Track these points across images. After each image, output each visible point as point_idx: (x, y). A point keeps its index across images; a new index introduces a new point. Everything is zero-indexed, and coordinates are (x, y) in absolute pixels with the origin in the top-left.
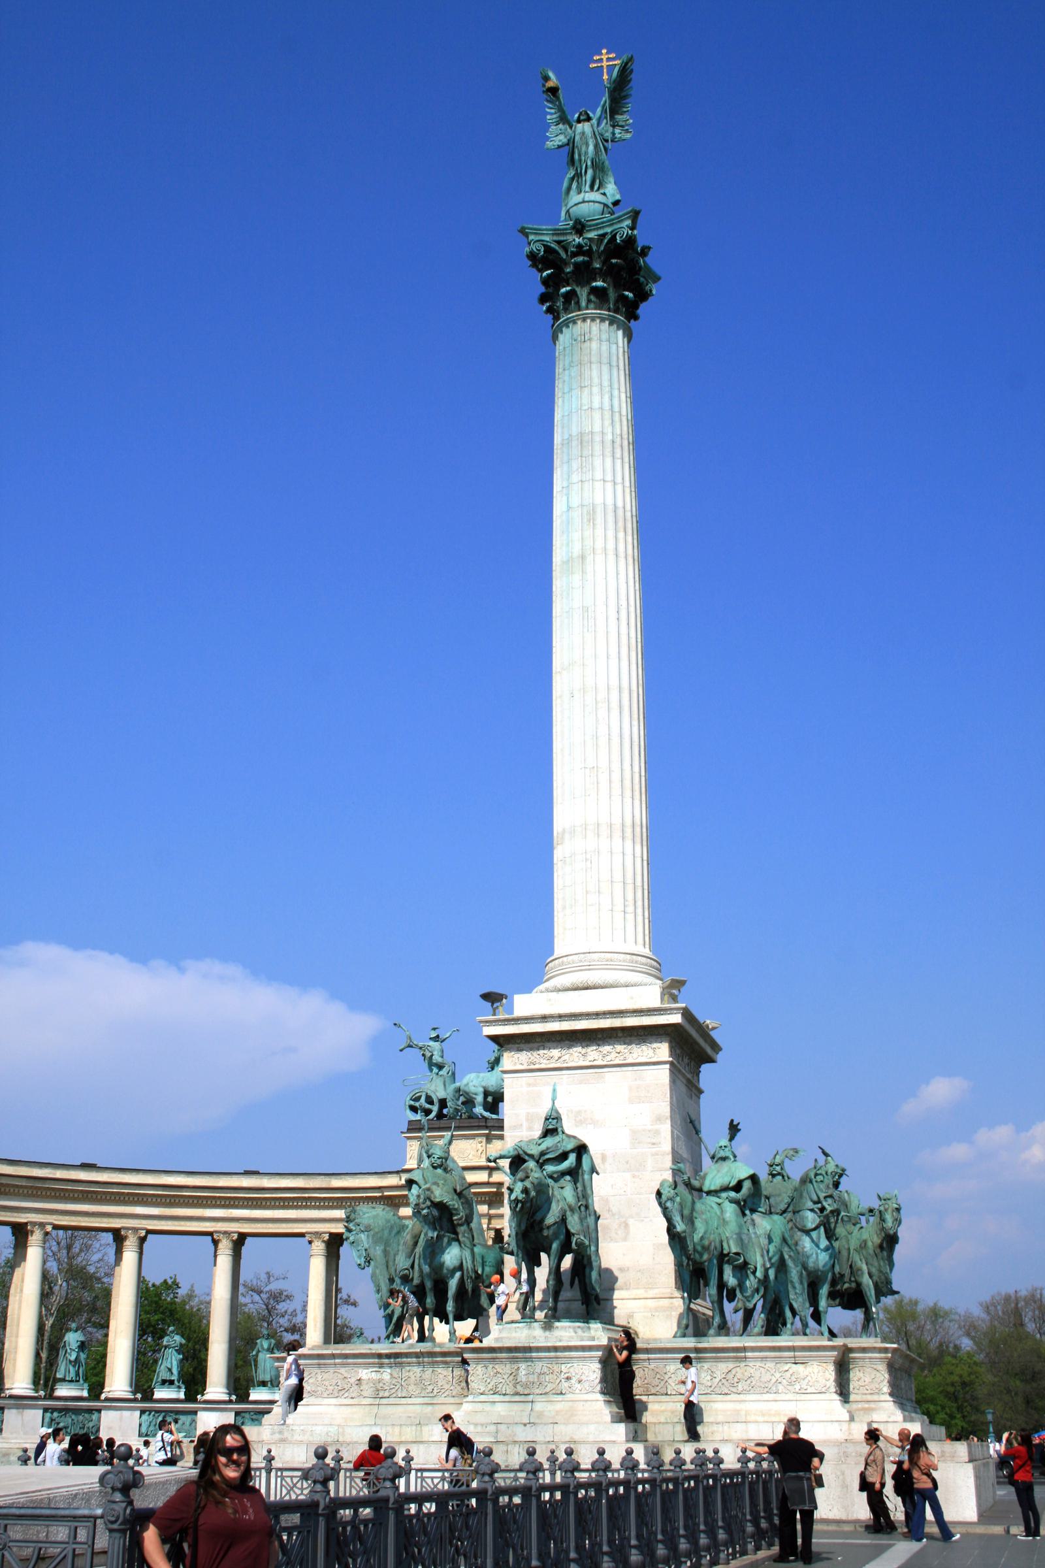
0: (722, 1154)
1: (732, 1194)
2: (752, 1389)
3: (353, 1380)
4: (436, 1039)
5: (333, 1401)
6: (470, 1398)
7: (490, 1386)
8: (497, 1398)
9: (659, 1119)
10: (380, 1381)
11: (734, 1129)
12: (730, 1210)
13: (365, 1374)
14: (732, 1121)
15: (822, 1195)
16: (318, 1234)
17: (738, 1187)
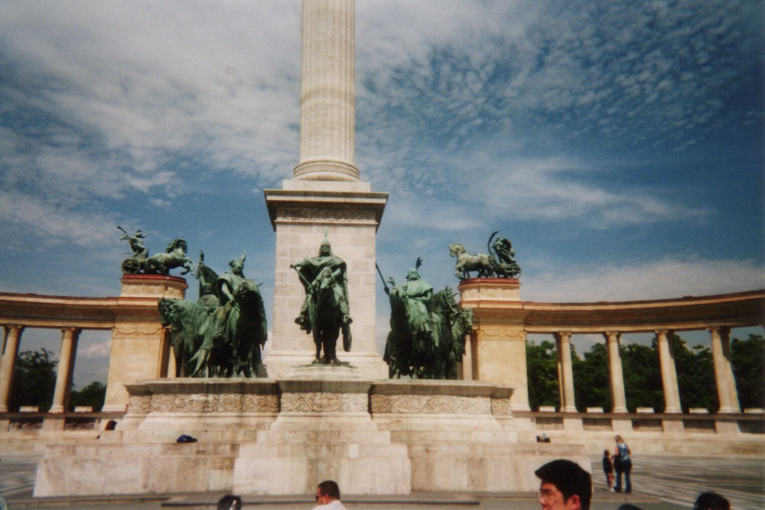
0: (414, 276)
1: (424, 298)
2: (444, 410)
3: (187, 401)
4: (139, 236)
5: (172, 414)
6: (282, 413)
7: (296, 406)
8: (301, 413)
9: (368, 256)
10: (206, 402)
11: (419, 263)
12: (423, 308)
13: (195, 397)
14: (419, 258)
15: (450, 305)
16: (69, 328)
17: (425, 294)
